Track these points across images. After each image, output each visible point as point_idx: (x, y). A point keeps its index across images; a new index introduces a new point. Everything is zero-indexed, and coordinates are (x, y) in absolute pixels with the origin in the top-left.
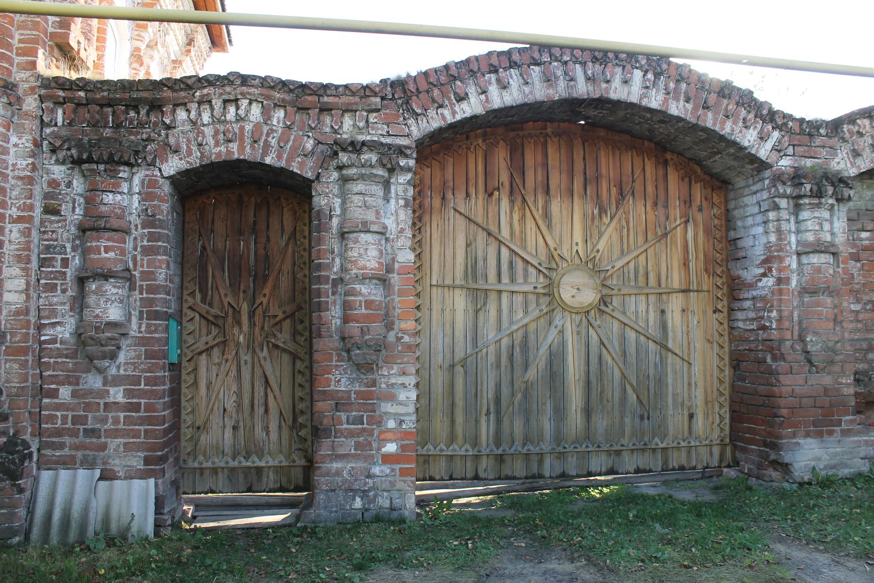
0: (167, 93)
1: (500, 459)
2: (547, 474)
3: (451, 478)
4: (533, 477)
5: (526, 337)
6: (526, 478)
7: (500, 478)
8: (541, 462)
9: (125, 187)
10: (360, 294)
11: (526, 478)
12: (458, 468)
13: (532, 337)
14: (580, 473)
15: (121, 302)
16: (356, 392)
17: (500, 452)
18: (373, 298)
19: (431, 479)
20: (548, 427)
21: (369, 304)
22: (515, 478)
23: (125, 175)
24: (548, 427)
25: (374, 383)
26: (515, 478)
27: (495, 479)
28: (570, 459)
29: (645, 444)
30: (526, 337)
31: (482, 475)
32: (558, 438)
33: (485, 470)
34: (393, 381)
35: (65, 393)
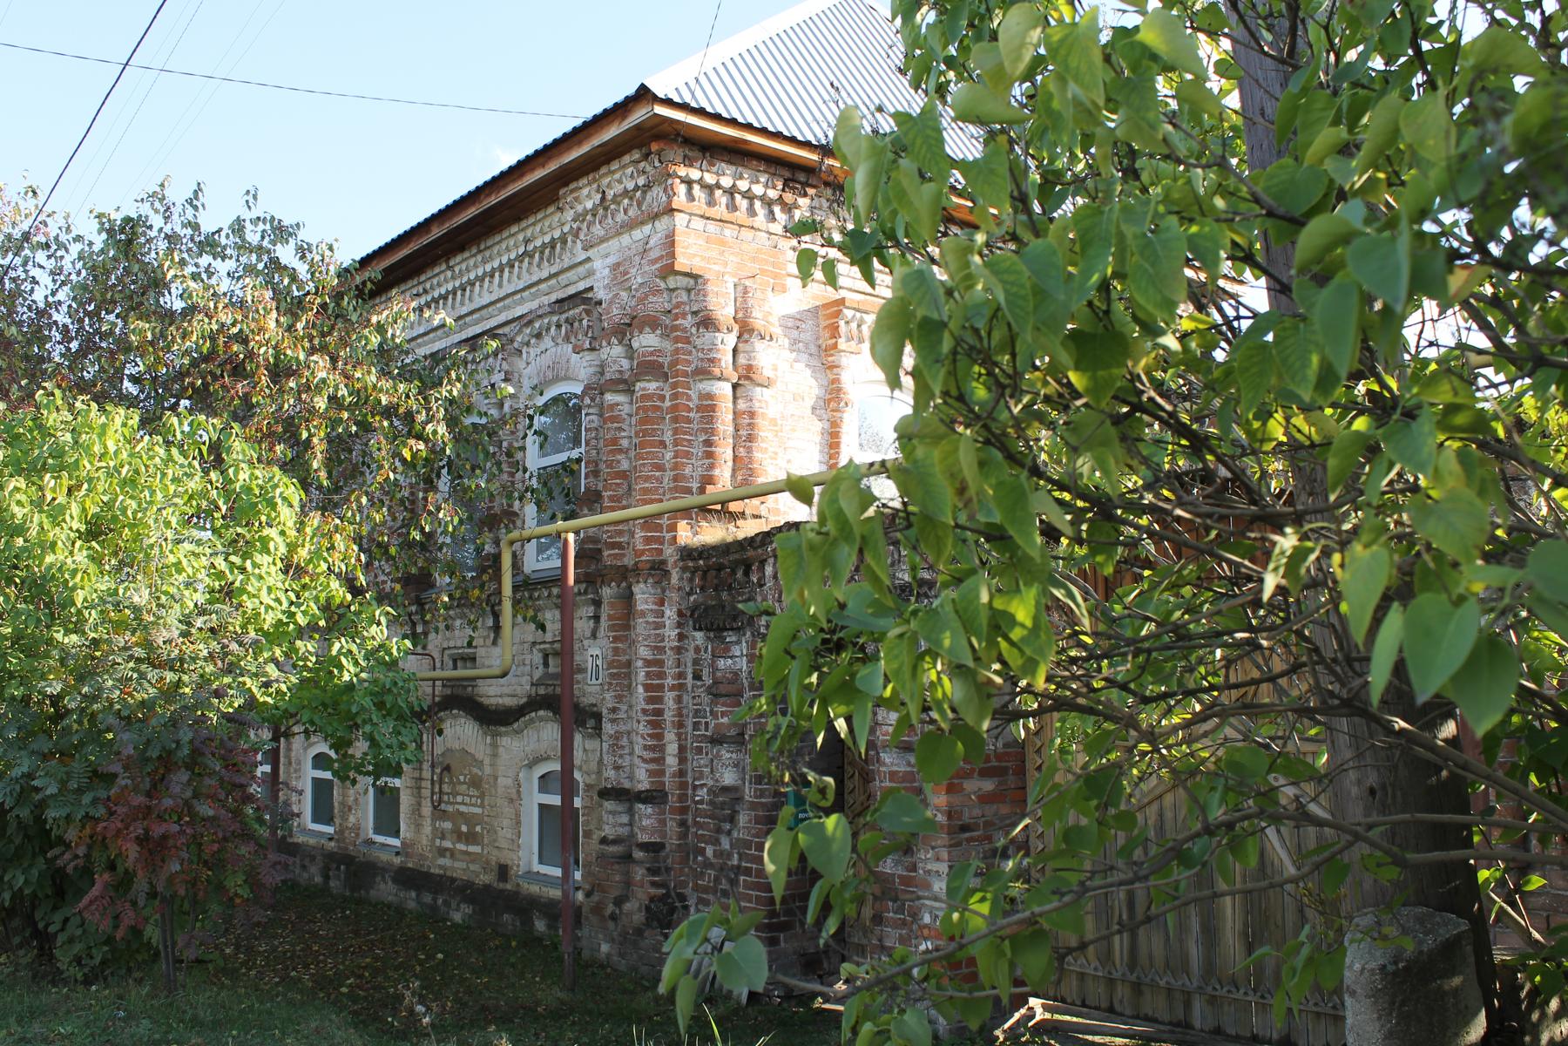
0: (750, 553)
1: (1137, 988)
2: (1197, 1024)
3: (1084, 1005)
4: (1178, 1024)
5: (1161, 815)
6: (1171, 1023)
7: (1137, 1017)
8: (1188, 1005)
9: (736, 651)
10: (884, 764)
11: (1171, 1023)
12: (1097, 993)
13: (1169, 815)
14: (1241, 1033)
15: (736, 766)
16: (900, 877)
17: (1133, 978)
18: (895, 768)
19: (1063, 1001)
20: (1195, 952)
21: (893, 775)
22: (1156, 1021)
23: (734, 639)
24: (1195, 952)
25: (914, 868)
26: (1156, 1021)
27: (1133, 1017)
28: (1226, 1008)
29: (1334, 1007)
30: (1161, 815)
31: (1118, 1007)
32: (1209, 968)
33: (1121, 1001)
34: (929, 867)
35: (709, 851)
